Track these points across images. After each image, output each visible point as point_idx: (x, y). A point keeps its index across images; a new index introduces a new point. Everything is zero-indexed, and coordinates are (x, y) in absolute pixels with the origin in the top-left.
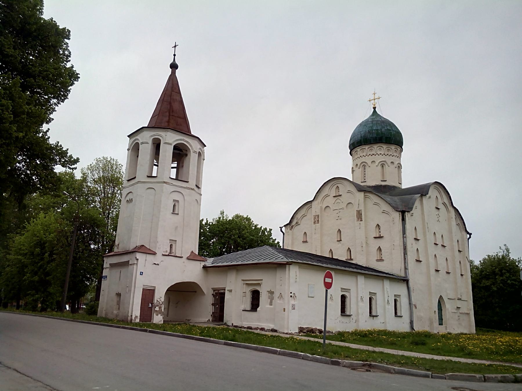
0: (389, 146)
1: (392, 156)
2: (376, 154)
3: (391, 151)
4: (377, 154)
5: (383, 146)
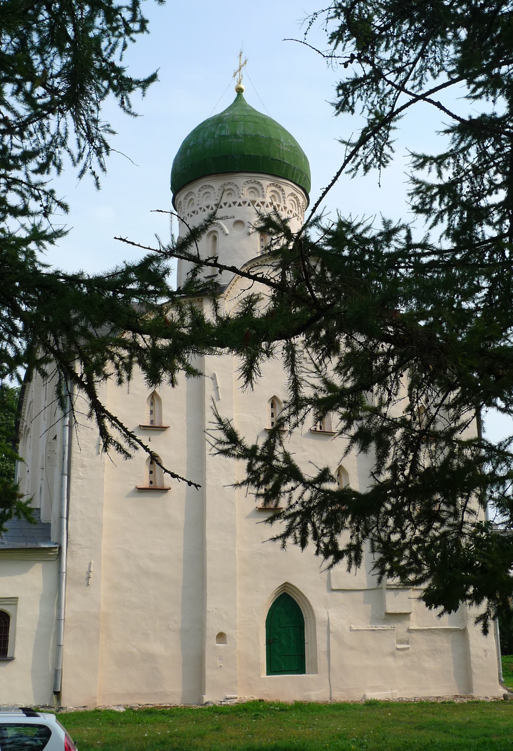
0: (229, 181)
1: (237, 204)
2: (199, 210)
3: (237, 193)
4: (201, 209)
5: (212, 184)
